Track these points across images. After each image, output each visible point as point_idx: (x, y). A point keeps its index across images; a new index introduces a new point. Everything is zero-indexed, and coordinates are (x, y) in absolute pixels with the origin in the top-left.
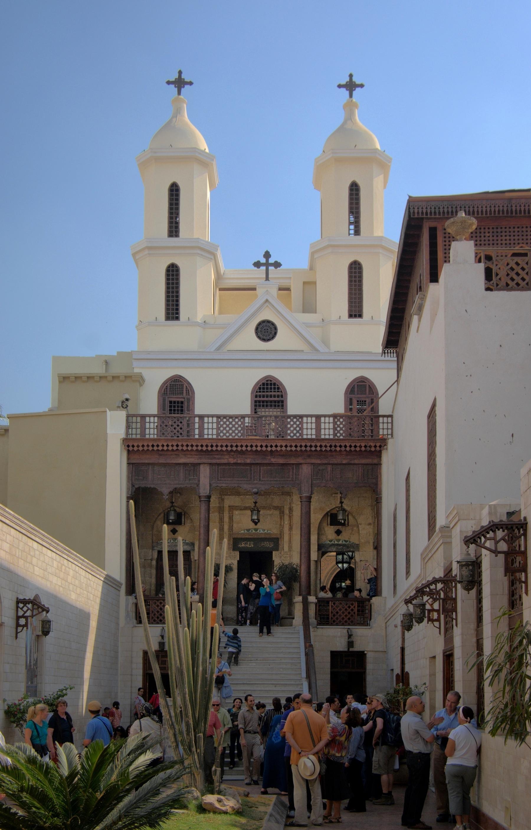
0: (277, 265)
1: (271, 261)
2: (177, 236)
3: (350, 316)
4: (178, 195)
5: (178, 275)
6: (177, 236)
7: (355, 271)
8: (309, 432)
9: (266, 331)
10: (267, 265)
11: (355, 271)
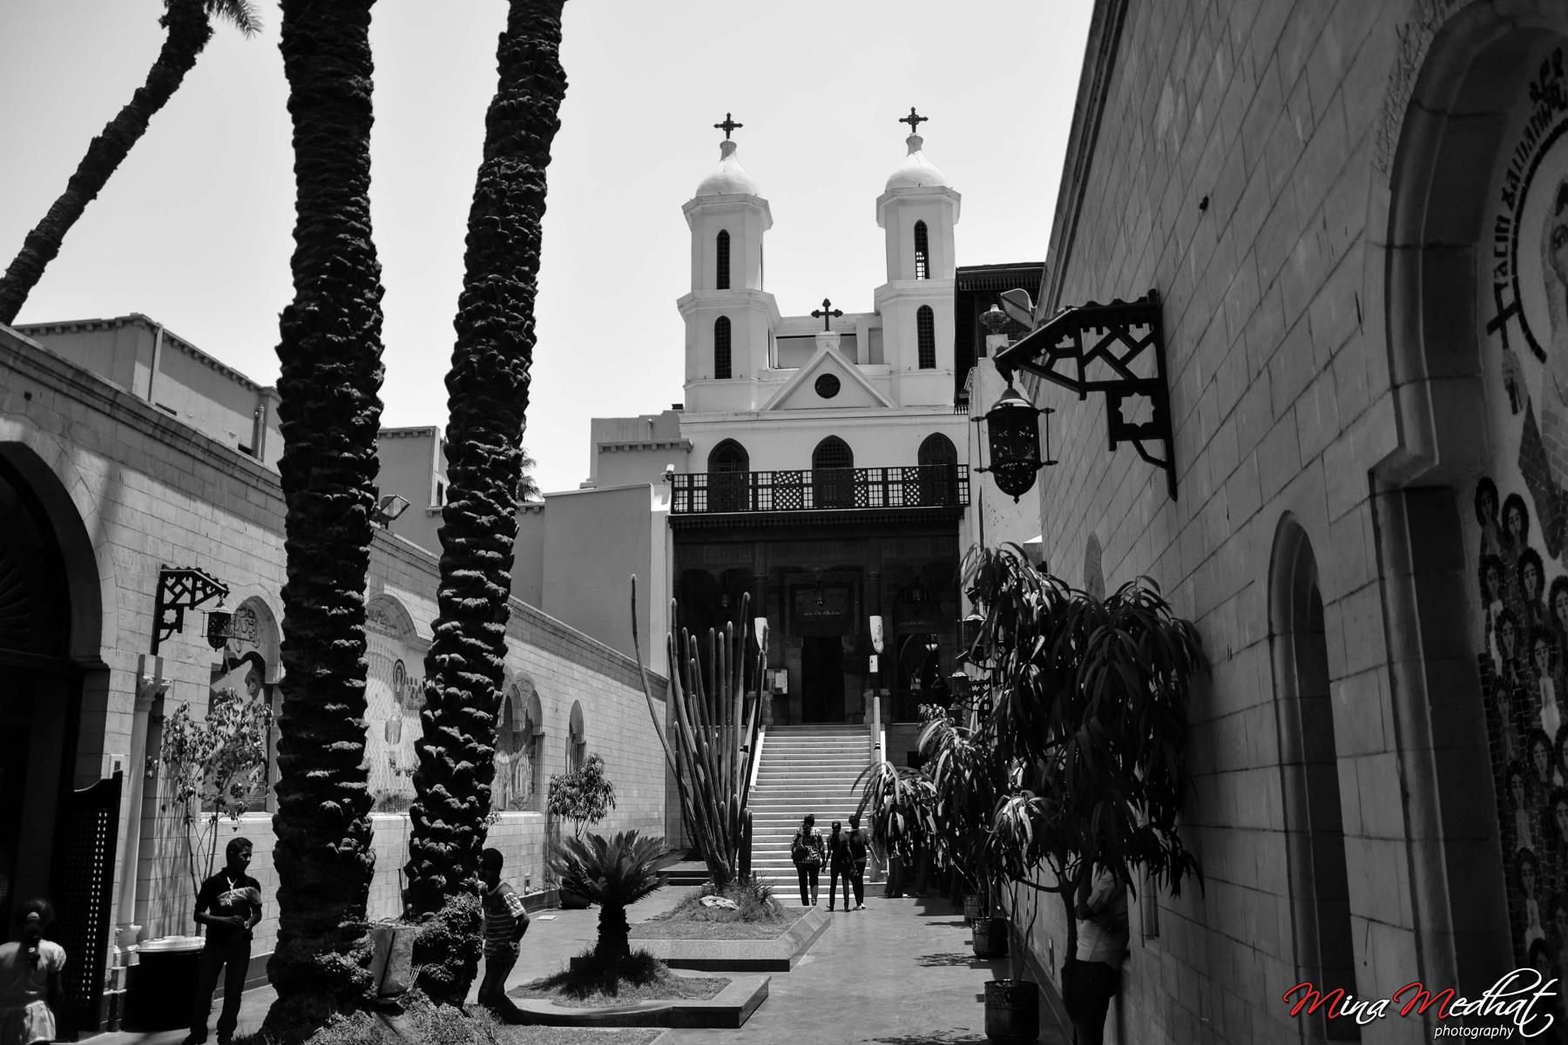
0: (838, 313)
1: (831, 309)
2: (727, 287)
3: (922, 366)
4: (728, 244)
5: (729, 329)
6: (727, 287)
7: (925, 317)
8: (876, 498)
9: (828, 386)
10: (827, 314)
11: (925, 317)
